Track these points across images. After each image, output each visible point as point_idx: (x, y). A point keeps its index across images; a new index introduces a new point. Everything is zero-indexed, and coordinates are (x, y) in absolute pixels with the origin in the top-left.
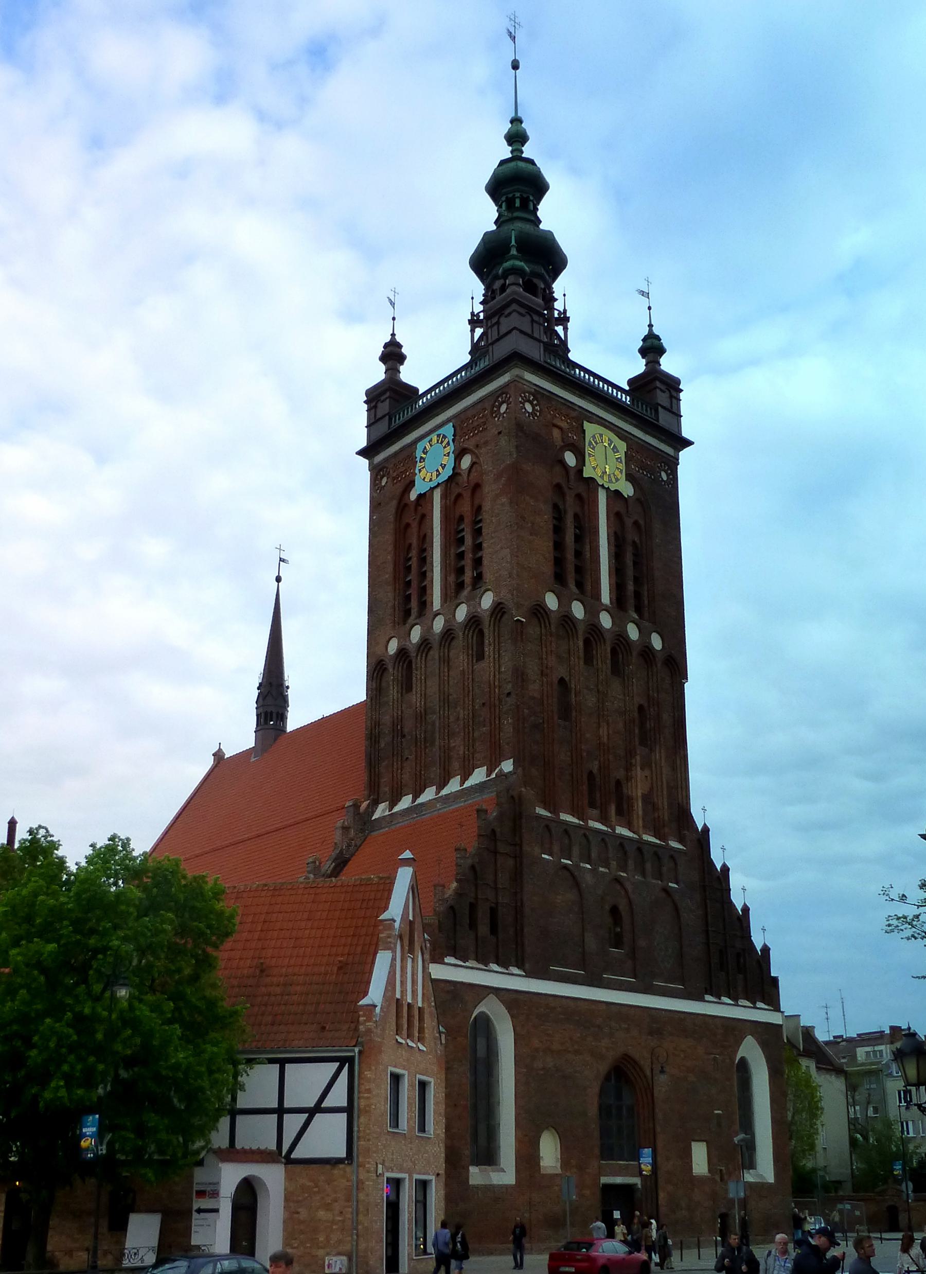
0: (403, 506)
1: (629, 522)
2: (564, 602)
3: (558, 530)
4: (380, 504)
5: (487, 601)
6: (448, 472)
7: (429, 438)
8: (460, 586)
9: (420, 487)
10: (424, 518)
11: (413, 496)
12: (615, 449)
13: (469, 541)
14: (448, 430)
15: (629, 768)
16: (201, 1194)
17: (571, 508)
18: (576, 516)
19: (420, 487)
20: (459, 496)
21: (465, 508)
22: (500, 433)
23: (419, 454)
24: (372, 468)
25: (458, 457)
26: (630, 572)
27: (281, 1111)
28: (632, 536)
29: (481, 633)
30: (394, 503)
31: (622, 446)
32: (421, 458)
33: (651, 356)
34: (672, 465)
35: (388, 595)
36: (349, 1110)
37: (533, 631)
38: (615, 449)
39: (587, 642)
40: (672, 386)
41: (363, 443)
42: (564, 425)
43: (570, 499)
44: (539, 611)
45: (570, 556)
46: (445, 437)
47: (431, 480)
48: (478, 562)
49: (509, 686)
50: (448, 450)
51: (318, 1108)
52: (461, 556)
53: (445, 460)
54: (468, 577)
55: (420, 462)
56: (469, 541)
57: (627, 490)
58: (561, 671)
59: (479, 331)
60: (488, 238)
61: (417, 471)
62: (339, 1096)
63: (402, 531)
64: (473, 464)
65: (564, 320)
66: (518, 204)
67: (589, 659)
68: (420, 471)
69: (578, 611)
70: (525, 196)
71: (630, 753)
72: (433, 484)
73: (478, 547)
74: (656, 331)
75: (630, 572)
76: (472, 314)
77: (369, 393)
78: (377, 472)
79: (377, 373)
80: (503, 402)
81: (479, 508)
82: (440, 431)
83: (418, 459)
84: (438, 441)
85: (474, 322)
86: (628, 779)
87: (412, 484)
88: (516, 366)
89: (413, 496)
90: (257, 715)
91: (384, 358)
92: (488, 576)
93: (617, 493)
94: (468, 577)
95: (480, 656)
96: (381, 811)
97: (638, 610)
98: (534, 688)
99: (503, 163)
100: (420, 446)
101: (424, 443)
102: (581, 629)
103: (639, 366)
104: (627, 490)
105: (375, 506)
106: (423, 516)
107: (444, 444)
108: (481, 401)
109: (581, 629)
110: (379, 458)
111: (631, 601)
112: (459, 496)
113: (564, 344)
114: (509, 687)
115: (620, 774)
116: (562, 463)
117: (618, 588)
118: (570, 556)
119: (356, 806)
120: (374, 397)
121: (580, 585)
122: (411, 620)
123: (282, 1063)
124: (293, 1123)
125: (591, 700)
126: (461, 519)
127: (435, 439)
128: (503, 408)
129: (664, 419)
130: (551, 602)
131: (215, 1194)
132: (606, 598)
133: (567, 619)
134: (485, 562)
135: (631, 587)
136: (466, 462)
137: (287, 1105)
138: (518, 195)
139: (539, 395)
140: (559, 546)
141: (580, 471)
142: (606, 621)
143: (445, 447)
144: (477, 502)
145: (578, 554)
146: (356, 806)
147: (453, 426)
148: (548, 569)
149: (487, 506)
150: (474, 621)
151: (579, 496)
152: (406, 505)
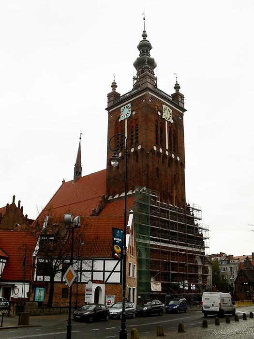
1: (172, 129)
2: (158, 149)
3: (157, 131)
5: (139, 147)
6: (129, 115)
8: (132, 143)
9: (122, 118)
10: (123, 126)
12: (169, 112)
13: (134, 133)
14: (129, 105)
15: (172, 189)
16: (87, 290)
17: (159, 125)
18: (161, 128)
19: (122, 118)
20: (132, 121)
21: (134, 124)
23: (121, 110)
24: (109, 113)
25: (132, 112)
26: (173, 142)
27: (104, 271)
28: (173, 133)
29: (138, 156)
31: (171, 111)
33: (177, 89)
34: (182, 115)
35: (112, 144)
36: (120, 272)
37: (151, 155)
38: (169, 112)
39: (163, 158)
40: (182, 97)
41: (107, 107)
42: (158, 105)
43: (159, 123)
44: (153, 150)
45: (159, 137)
48: (137, 138)
49: (145, 169)
51: (113, 271)
52: (132, 136)
54: (134, 141)
56: (134, 133)
57: (172, 121)
58: (157, 166)
59: (135, 81)
60: (138, 59)
62: (118, 268)
63: (117, 129)
64: (136, 114)
65: (156, 79)
67: (163, 163)
69: (161, 150)
71: (172, 186)
72: (125, 118)
73: (137, 134)
74: (178, 83)
75: (173, 142)
78: (109, 113)
79: (110, 90)
81: (137, 125)
85: (134, 78)
86: (172, 192)
87: (120, 117)
89: (120, 121)
90: (75, 172)
91: (112, 86)
92: (140, 141)
93: (170, 122)
94: (134, 141)
95: (137, 161)
96: (110, 198)
97: (174, 151)
98: (151, 169)
99: (141, 41)
100: (122, 108)
102: (162, 155)
103: (174, 91)
104: (172, 121)
105: (110, 122)
106: (122, 126)
109: (162, 155)
110: (110, 111)
111: (173, 149)
112: (132, 121)
113: (156, 84)
114: (145, 169)
115: (170, 191)
116: (158, 115)
117: (170, 145)
118: (159, 137)
119: (104, 196)
120: (109, 96)
121: (161, 144)
122: (119, 151)
123: (104, 260)
124: (107, 274)
125: (163, 173)
126: (132, 127)
129: (180, 104)
130: (155, 148)
131: (91, 290)
132: (167, 148)
133: (158, 152)
134: (139, 138)
135: (173, 145)
136: (134, 113)
137: (105, 270)
139: (153, 98)
140: (157, 134)
141: (162, 117)
142: (167, 153)
144: (137, 123)
145: (161, 137)
146: (104, 196)
148: (154, 140)
149: (139, 124)
150: (136, 152)
151: (161, 122)
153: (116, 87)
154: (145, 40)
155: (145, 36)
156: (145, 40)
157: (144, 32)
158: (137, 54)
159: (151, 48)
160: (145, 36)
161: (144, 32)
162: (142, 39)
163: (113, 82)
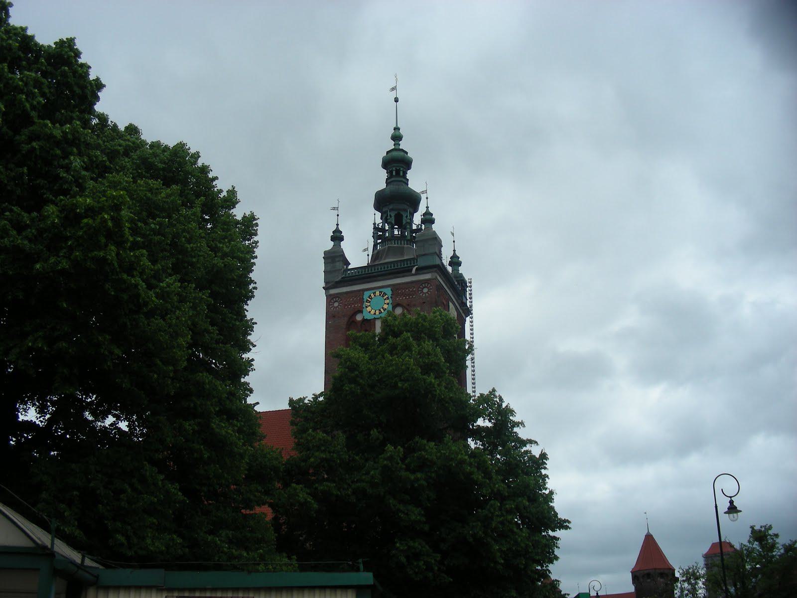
0: (351, 323)
4: (334, 316)
7: (374, 291)
11: (359, 318)
14: (388, 292)
22: (424, 303)
23: (366, 297)
30: (346, 319)
47: (375, 314)
50: (387, 301)
53: (386, 306)
55: (367, 302)
61: (364, 306)
66: (401, 174)
68: (367, 307)
70: (404, 170)
76: (374, 224)
77: (325, 253)
78: (330, 299)
79: (330, 245)
80: (425, 287)
82: (381, 290)
83: (365, 300)
84: (380, 295)
88: (436, 271)
89: (359, 318)
91: (333, 239)
100: (366, 294)
101: (371, 293)
107: (385, 298)
108: (412, 282)
110: (333, 291)
127: (378, 293)
128: (425, 290)
138: (402, 169)
139: (439, 287)
143: (385, 299)
147: (391, 290)
152: (353, 321)
153: (342, 239)
155: (397, 138)
157: (397, 129)
158: (379, 180)
159: (409, 168)
160: (397, 138)
161: (397, 129)
162: (391, 145)
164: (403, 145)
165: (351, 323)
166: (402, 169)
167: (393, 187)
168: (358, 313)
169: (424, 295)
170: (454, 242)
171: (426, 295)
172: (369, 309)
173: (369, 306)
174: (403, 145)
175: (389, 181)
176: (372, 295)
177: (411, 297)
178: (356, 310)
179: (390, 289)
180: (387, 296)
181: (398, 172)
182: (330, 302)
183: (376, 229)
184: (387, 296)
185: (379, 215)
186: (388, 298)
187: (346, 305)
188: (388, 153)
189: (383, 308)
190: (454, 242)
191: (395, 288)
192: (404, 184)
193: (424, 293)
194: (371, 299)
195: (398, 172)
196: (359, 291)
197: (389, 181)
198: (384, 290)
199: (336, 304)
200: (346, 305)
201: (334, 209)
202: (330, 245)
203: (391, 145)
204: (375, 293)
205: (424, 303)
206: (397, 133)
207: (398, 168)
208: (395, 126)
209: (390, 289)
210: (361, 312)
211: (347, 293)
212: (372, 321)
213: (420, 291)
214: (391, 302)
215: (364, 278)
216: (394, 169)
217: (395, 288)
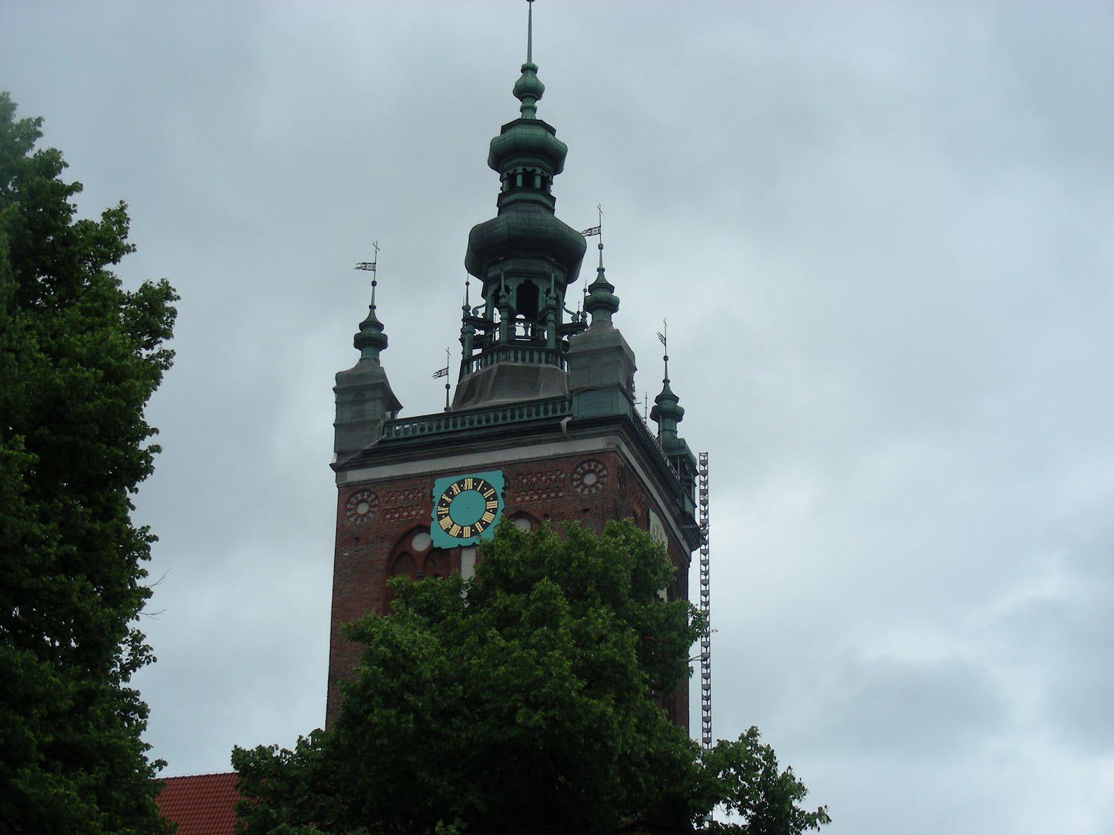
0: (400, 557)
4: (357, 539)
11: (420, 544)
14: (496, 480)
22: (586, 510)
30: (386, 546)
32: (442, 501)
46: (487, 486)
47: (460, 536)
50: (492, 505)
53: (488, 517)
61: (434, 515)
68: (440, 517)
70: (546, 174)
72: (463, 542)
76: (466, 308)
77: (340, 377)
78: (349, 495)
79: (351, 358)
80: (590, 471)
82: (478, 475)
83: (437, 500)
84: (475, 488)
88: (616, 432)
89: (420, 544)
91: (360, 342)
100: (440, 486)
101: (451, 481)
107: (486, 495)
108: (557, 458)
110: (356, 476)
127: (469, 483)
128: (590, 479)
139: (626, 472)
143: (488, 500)
154: (528, 121)
155: (528, 91)
156: (528, 121)
157: (529, 69)
160: (528, 91)
161: (529, 69)
162: (512, 110)
163: (364, 315)
164: (544, 109)
165: (400, 557)
166: (539, 171)
167: (516, 217)
168: (415, 535)
169: (586, 492)
170: (666, 358)
171: (590, 491)
172: (446, 522)
173: (446, 515)
174: (544, 109)
175: (505, 201)
176: (455, 488)
177: (553, 495)
178: (415, 524)
179: (499, 473)
180: (491, 492)
181: (529, 178)
182: (348, 502)
183: (469, 320)
184: (491, 492)
185: (477, 285)
186: (494, 497)
187: (388, 511)
188: (505, 129)
189: (481, 521)
190: (666, 358)
191: (512, 471)
192: (542, 210)
193: (586, 486)
194: (452, 497)
195: (529, 178)
196: (422, 476)
197: (505, 201)
198: (484, 476)
199: (363, 509)
200: (388, 511)
201: (365, 266)
202: (351, 358)
203: (512, 110)
204: (462, 482)
205: (586, 510)
206: (530, 80)
207: (529, 169)
208: (525, 62)
209: (499, 473)
210: (426, 529)
211: (392, 480)
212: (452, 552)
213: (577, 480)
214: (502, 506)
215: (435, 444)
216: (520, 170)
217: (512, 471)
